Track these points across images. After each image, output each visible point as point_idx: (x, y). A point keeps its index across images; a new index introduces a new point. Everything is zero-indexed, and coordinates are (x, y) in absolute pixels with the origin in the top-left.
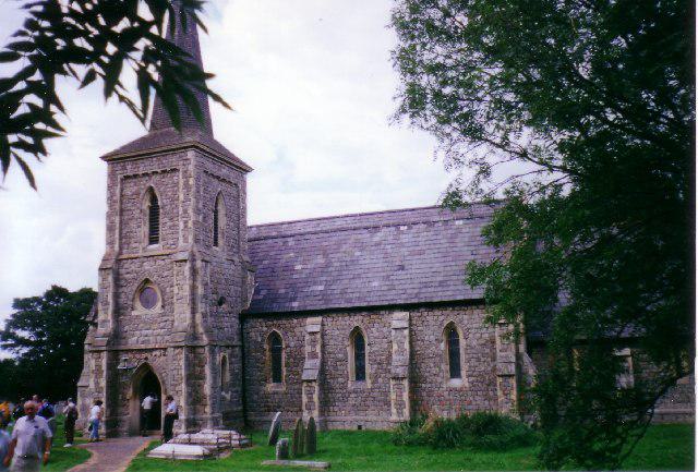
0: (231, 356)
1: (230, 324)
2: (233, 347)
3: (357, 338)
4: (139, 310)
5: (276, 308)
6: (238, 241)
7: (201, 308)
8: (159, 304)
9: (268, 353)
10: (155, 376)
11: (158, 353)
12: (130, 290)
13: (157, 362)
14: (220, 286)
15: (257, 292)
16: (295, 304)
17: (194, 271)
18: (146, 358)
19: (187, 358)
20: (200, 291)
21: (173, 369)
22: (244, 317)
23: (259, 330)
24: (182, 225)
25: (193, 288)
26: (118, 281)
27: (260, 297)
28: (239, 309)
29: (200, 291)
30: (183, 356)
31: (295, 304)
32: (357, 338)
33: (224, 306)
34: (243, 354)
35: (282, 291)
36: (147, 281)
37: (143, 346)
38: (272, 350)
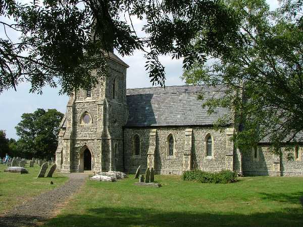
0: (119, 144)
1: (119, 131)
2: (120, 140)
3: (170, 139)
4: (83, 123)
5: (137, 125)
6: (122, 97)
7: (108, 123)
8: (91, 122)
9: (133, 143)
10: (89, 151)
11: (90, 141)
12: (79, 115)
13: (90, 145)
14: (115, 115)
15: (130, 117)
16: (146, 123)
17: (105, 109)
18: (86, 143)
19: (102, 144)
20: (108, 117)
21: (96, 148)
22: (124, 128)
23: (131, 133)
24: (100, 91)
25: (105, 116)
26: (75, 112)
27: (131, 120)
28: (123, 125)
29: (108, 117)
30: (101, 143)
31: (146, 123)
32: (170, 139)
33: (116, 123)
34: (124, 143)
35: (141, 118)
36: (86, 112)
37: (84, 138)
38: (135, 142)
